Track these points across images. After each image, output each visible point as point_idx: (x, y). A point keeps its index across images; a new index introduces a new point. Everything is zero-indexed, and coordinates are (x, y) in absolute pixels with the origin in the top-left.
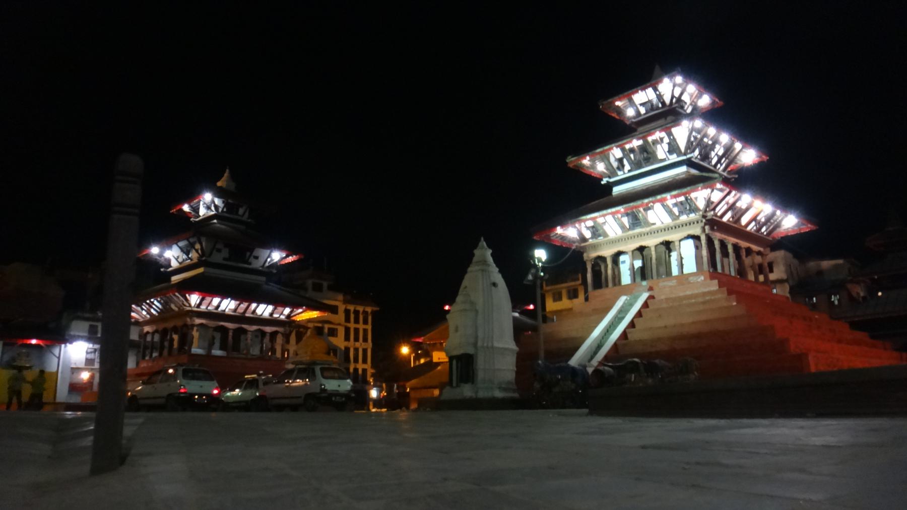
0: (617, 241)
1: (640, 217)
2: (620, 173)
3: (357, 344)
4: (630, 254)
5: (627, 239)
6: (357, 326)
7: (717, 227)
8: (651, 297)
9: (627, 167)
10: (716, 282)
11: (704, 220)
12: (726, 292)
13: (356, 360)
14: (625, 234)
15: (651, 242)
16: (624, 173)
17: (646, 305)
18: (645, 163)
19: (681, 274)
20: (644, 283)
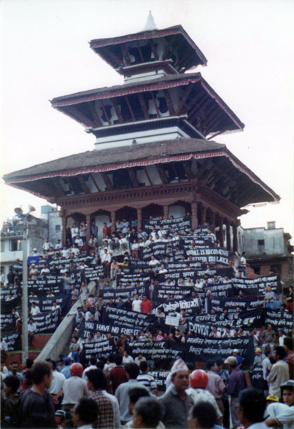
2: (106, 124)
4: (113, 215)
9: (115, 118)
15: (139, 204)
16: (110, 124)
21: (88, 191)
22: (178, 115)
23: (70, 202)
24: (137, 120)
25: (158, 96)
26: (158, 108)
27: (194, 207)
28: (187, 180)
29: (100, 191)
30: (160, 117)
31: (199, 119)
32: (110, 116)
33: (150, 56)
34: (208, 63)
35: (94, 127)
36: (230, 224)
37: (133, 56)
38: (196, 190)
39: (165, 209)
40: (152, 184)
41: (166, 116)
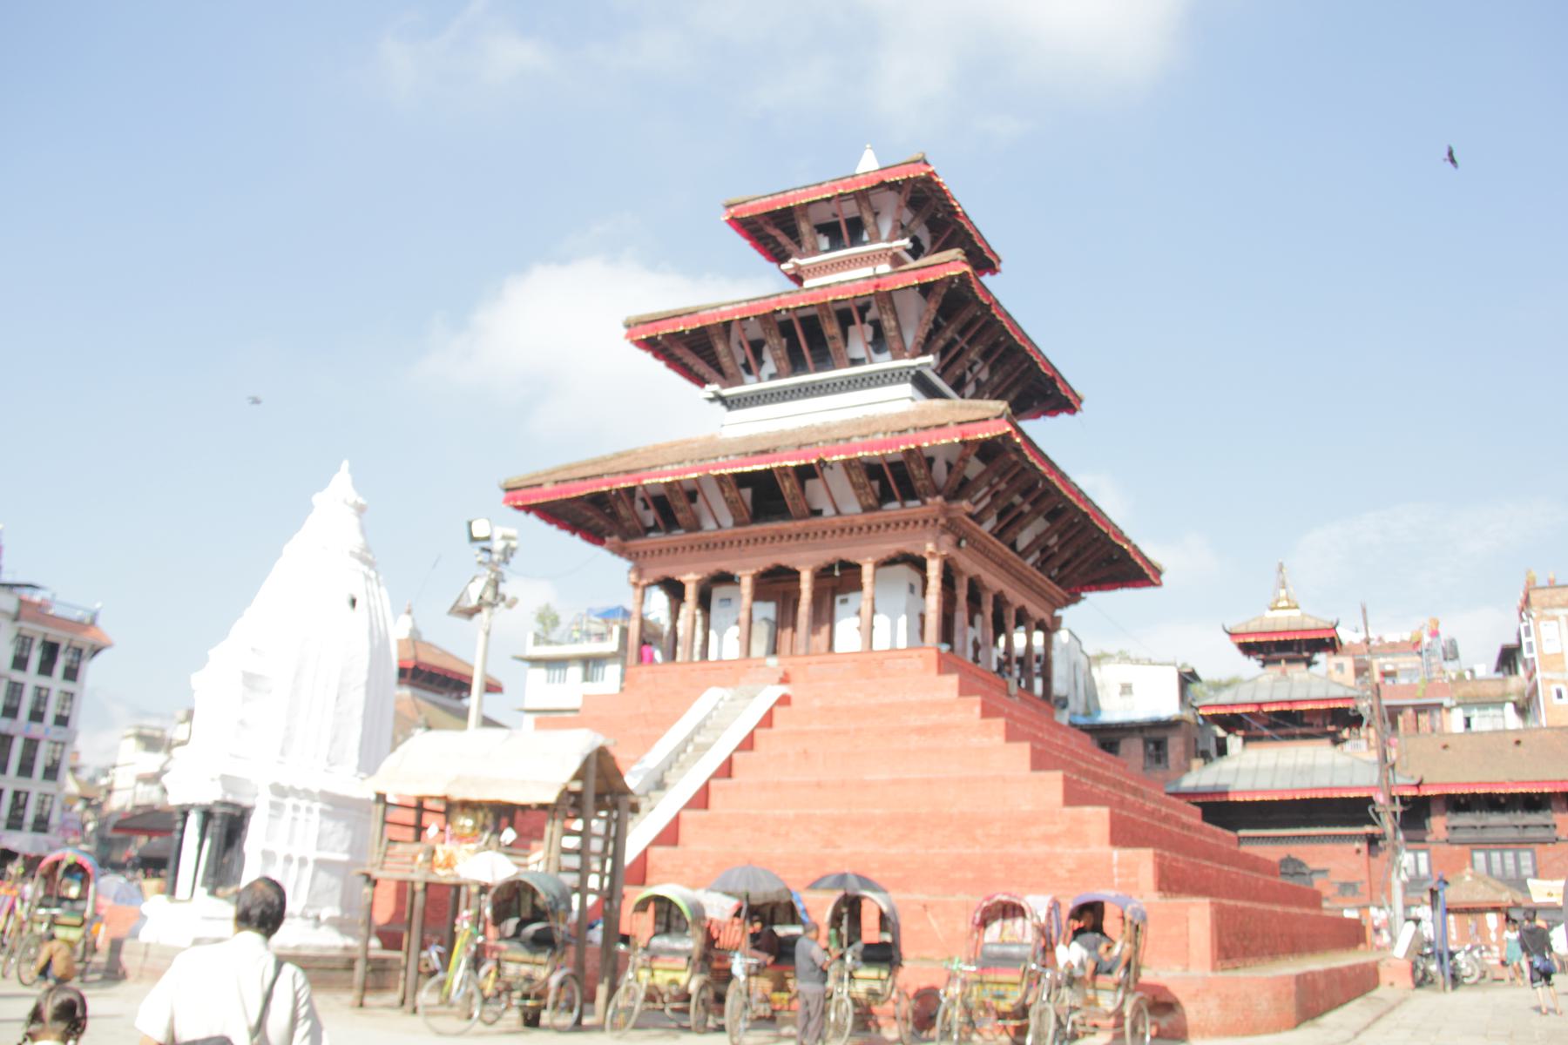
0: (720, 545)
1: (784, 487)
3: (36, 730)
5: (744, 542)
6: (44, 681)
7: (968, 543)
8: (784, 700)
9: (769, 367)
10: (953, 680)
11: (942, 521)
12: (977, 710)
13: (26, 769)
14: (740, 530)
16: (760, 380)
17: (767, 721)
18: (814, 362)
19: (866, 649)
20: (772, 662)
21: (696, 526)
22: (914, 356)
23: (653, 552)
24: (817, 370)
25: (870, 316)
26: (870, 343)
27: (934, 569)
28: (917, 503)
29: (719, 526)
30: (871, 362)
31: (969, 376)
32: (760, 362)
33: (862, 234)
34: (1002, 266)
35: (723, 387)
36: (1033, 625)
37: (825, 235)
38: (943, 526)
39: (867, 570)
40: (838, 513)
41: (884, 362)
